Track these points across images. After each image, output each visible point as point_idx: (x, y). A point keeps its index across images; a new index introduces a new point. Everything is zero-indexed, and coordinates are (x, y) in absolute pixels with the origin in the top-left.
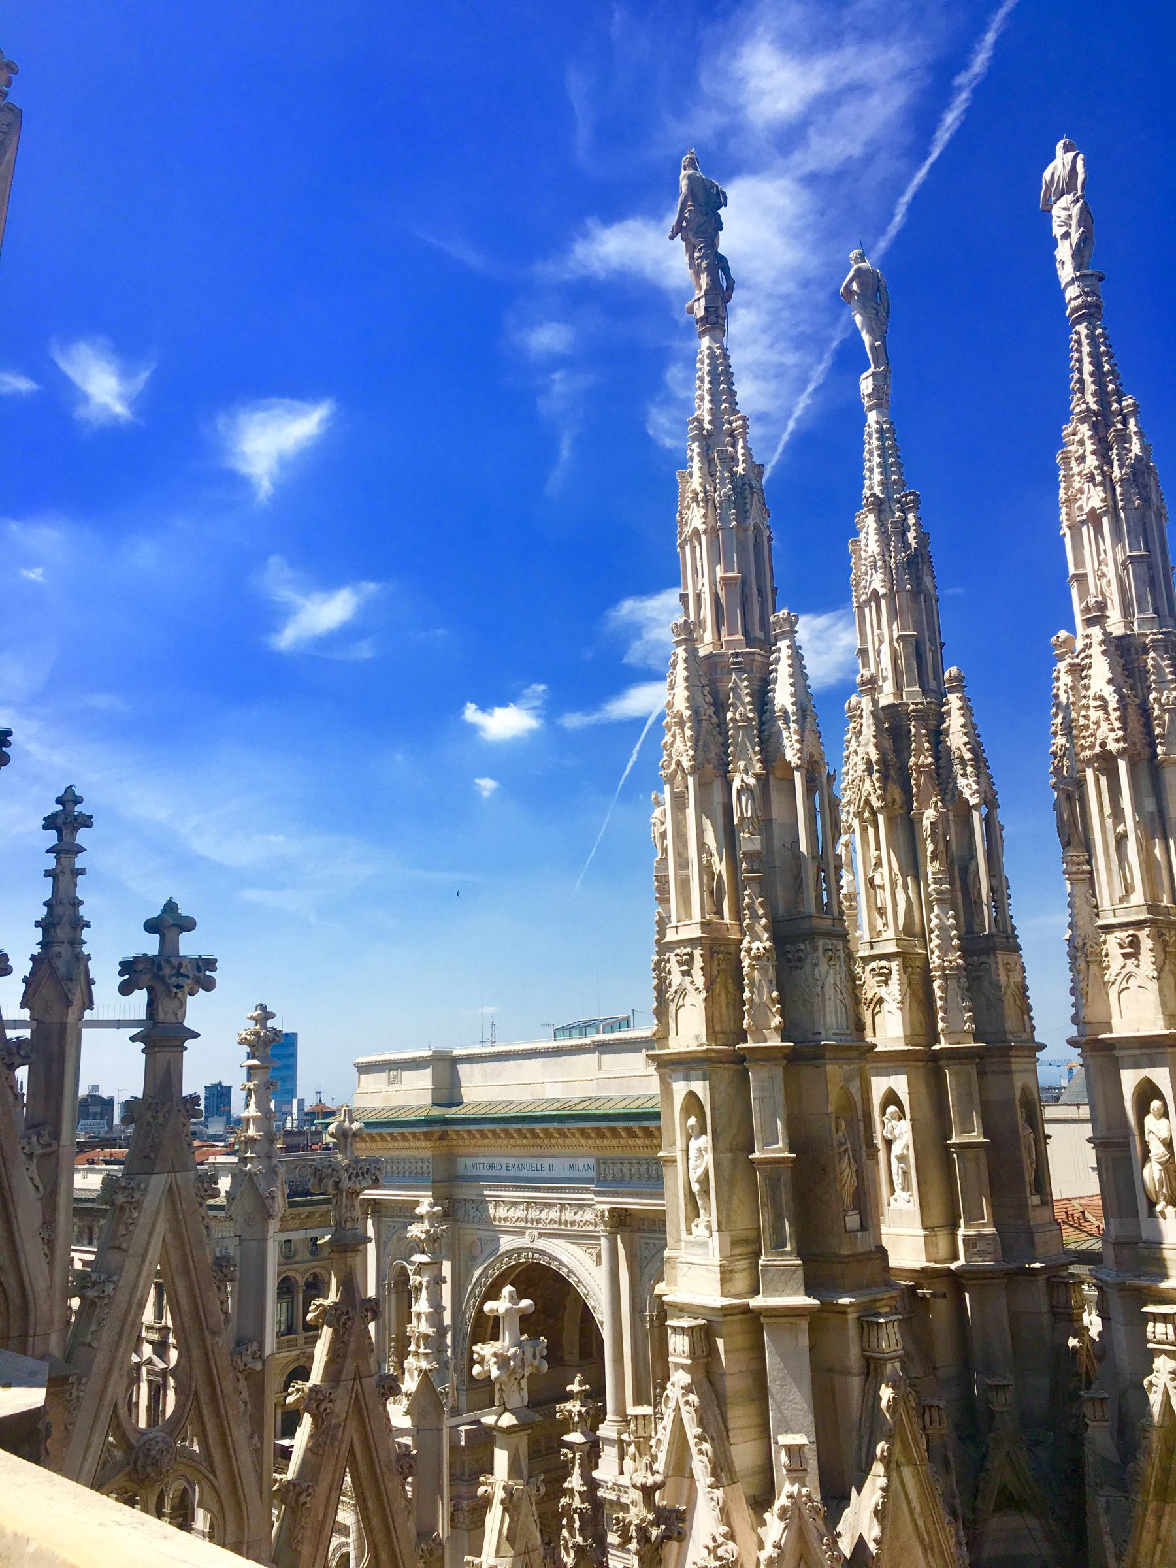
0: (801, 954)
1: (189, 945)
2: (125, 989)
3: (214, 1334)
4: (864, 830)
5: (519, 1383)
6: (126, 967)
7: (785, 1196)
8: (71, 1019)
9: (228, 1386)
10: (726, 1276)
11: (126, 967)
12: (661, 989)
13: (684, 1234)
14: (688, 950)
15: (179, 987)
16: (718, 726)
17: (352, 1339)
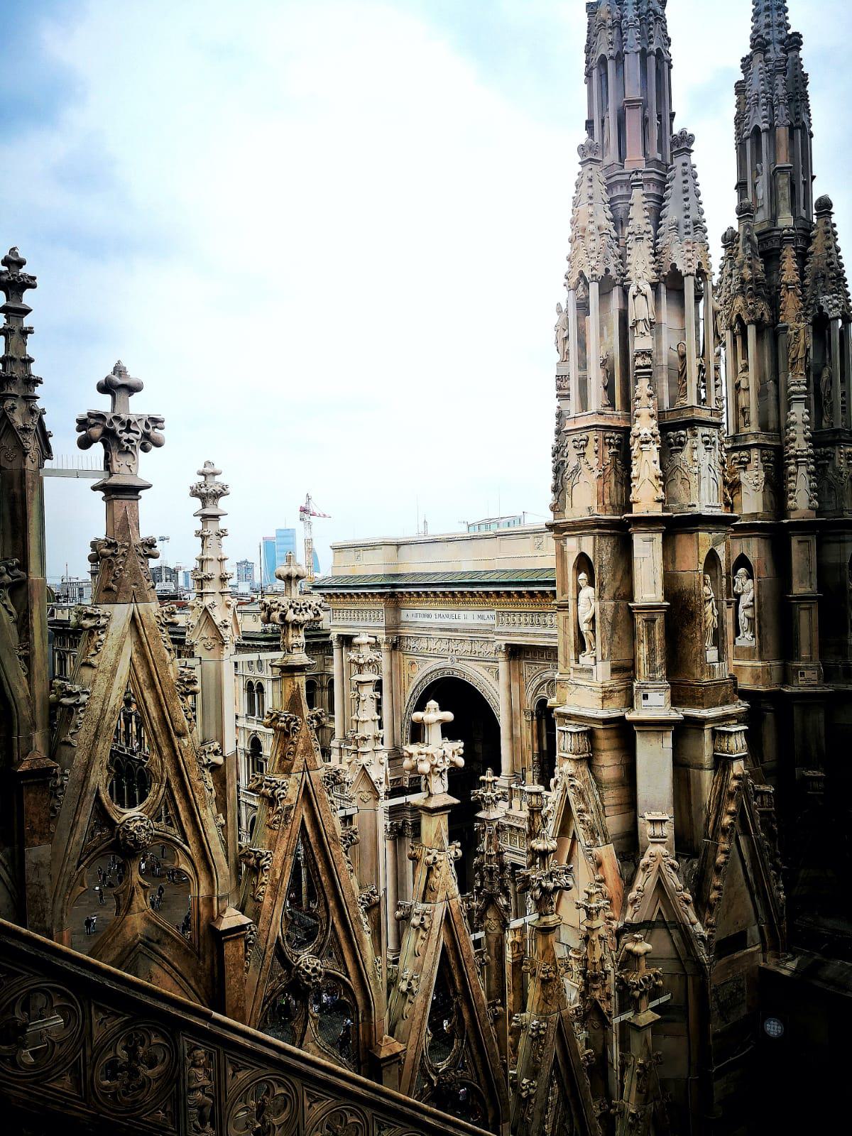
0: (682, 439)
1: (137, 406)
2: (85, 443)
3: (181, 735)
4: (735, 342)
5: (441, 776)
6: (82, 424)
7: (658, 634)
8: (30, 466)
9: (194, 776)
10: (607, 695)
11: (82, 424)
12: (558, 470)
13: (573, 663)
14: (584, 436)
15: (129, 441)
16: (617, 239)
17: (301, 740)
